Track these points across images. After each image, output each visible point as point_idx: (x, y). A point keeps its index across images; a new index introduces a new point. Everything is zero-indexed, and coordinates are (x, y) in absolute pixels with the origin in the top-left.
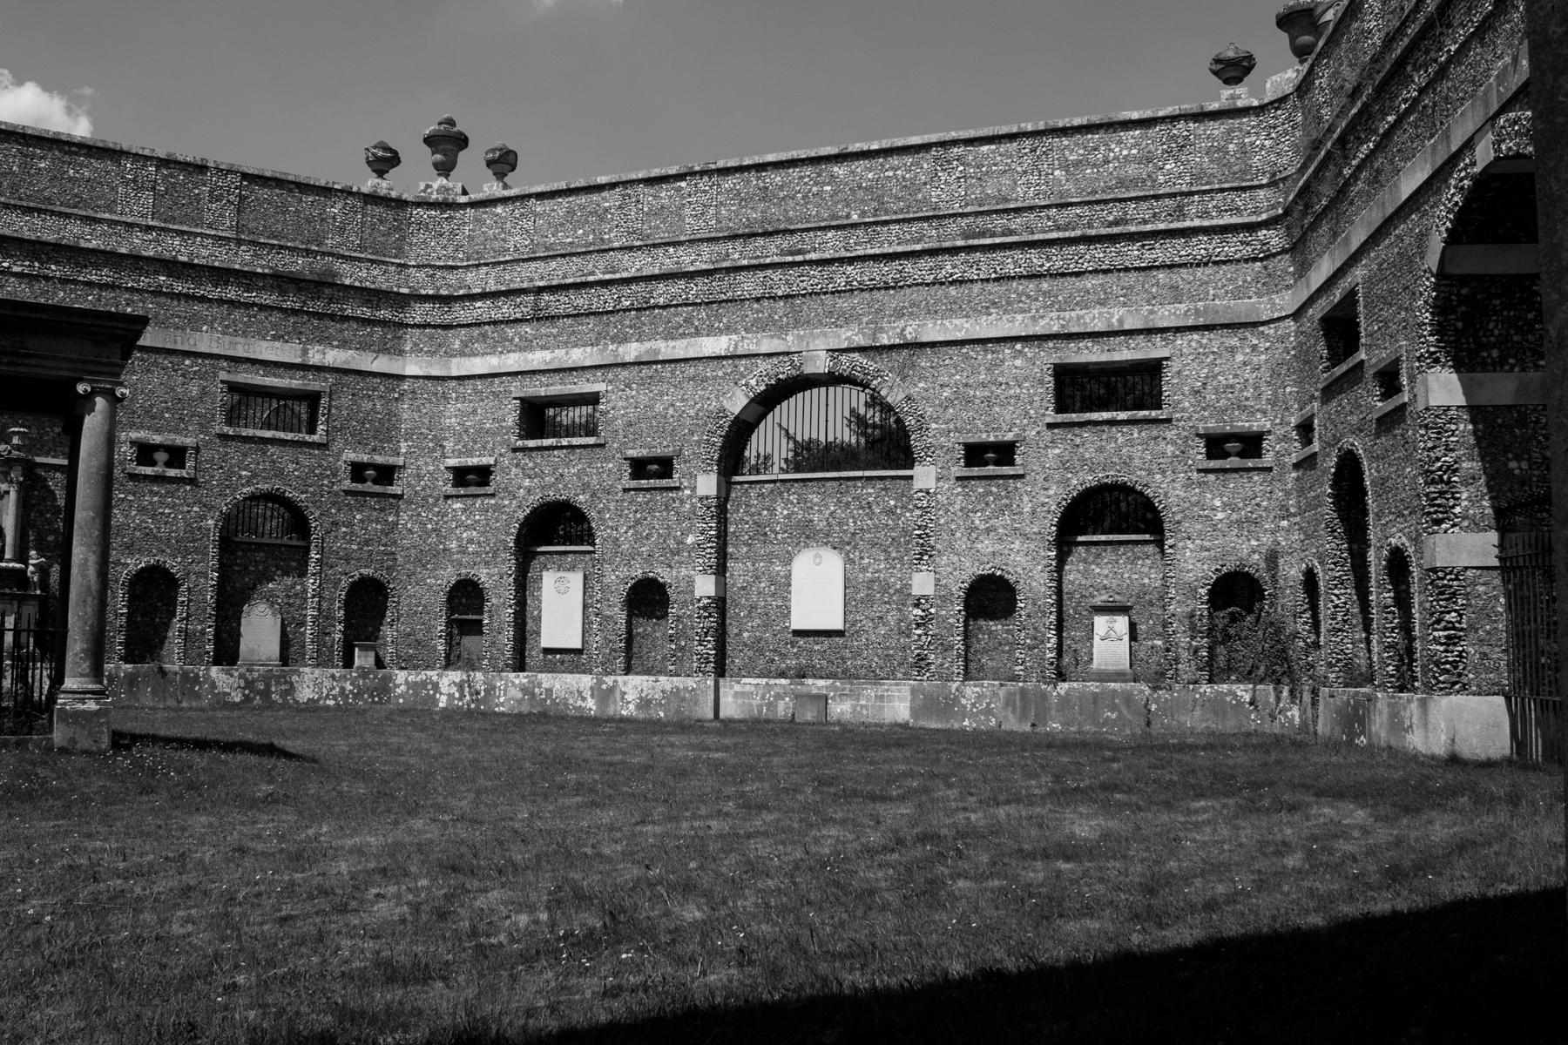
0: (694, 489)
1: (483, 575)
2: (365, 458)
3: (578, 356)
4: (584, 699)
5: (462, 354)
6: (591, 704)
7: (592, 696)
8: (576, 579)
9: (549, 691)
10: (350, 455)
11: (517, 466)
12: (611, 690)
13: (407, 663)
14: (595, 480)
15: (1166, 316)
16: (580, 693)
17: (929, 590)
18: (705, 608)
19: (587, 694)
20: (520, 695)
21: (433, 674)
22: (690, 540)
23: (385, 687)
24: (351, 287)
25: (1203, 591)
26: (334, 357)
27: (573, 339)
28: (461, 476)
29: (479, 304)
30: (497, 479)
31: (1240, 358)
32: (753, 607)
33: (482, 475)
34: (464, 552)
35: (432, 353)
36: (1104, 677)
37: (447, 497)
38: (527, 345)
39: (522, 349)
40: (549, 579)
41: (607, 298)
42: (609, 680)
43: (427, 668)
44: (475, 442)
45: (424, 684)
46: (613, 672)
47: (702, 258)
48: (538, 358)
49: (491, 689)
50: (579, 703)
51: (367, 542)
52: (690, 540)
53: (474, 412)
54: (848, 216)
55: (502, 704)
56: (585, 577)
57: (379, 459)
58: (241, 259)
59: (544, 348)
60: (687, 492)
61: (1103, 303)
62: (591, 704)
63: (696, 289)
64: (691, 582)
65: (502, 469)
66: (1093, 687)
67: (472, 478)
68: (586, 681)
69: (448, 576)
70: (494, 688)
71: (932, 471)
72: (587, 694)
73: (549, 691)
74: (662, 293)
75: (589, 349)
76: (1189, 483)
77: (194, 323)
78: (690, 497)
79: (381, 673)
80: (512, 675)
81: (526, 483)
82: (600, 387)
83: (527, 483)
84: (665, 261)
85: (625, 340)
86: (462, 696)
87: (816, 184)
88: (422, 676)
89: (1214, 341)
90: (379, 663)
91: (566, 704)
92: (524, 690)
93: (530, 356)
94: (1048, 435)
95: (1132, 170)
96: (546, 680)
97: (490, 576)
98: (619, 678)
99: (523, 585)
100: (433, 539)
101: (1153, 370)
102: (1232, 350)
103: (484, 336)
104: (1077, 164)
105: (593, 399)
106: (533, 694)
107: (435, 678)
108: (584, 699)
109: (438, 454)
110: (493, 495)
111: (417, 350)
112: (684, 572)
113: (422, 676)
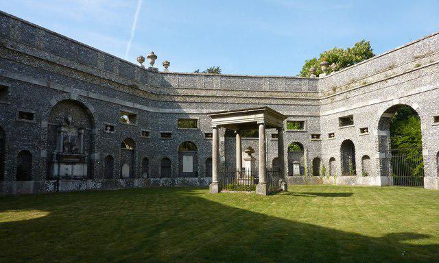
1: (170, 157)
6: (198, 183)
8: (191, 158)
9: (188, 182)
10: (142, 130)
15: (306, 113)
26: (138, 106)
28: (163, 135)
33: (170, 134)
36: (296, 175)
40: (185, 158)
41: (199, 100)
47: (219, 94)
58: (121, 80)
63: (218, 100)
67: (166, 135)
69: (160, 157)
73: (188, 182)
74: (211, 100)
77: (114, 96)
81: (180, 139)
84: (210, 93)
89: (313, 119)
92: (182, 181)
96: (187, 179)
99: (181, 159)
101: (302, 123)
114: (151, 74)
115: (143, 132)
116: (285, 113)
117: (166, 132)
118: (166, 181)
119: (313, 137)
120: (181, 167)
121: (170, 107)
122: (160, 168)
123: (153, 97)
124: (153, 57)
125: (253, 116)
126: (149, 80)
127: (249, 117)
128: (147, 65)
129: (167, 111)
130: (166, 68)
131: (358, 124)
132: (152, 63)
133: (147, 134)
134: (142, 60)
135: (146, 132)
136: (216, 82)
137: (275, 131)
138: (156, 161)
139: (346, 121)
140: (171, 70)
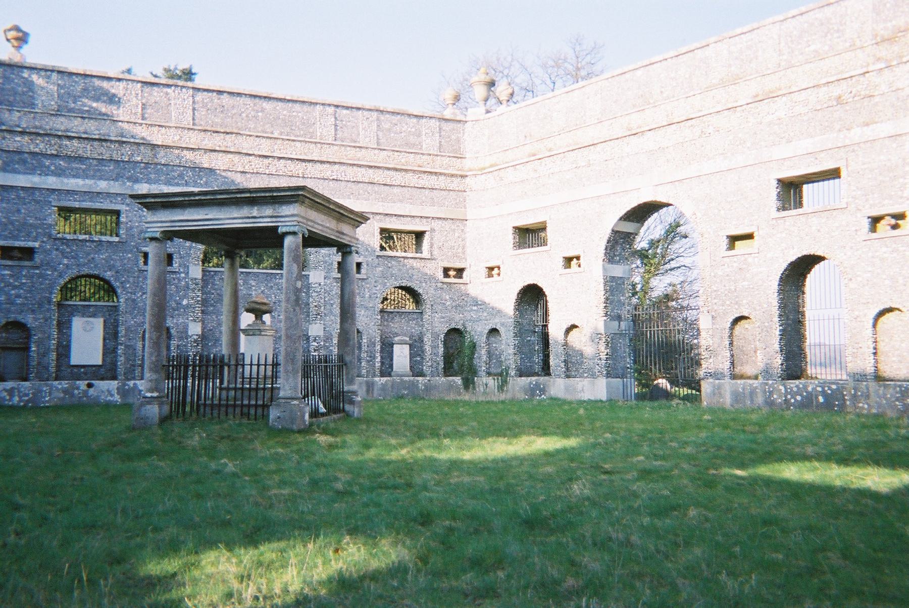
1: (29, 320)
3: (102, 185)
4: (112, 395)
6: (117, 398)
7: (118, 393)
8: (98, 324)
11: (57, 250)
14: (118, 264)
18: (195, 341)
20: (62, 395)
22: (185, 302)
27: (98, 174)
29: (18, 139)
30: (38, 258)
31: (457, 234)
33: (28, 253)
34: (12, 303)
39: (59, 175)
40: (78, 323)
46: (134, 378)
50: (109, 398)
52: (185, 302)
53: (18, 211)
54: (272, 133)
55: (47, 402)
56: (105, 322)
59: (74, 176)
60: (183, 275)
61: (401, 201)
62: (117, 398)
64: (186, 328)
68: (114, 384)
70: (41, 391)
71: (323, 274)
75: (112, 182)
78: (185, 278)
83: (65, 261)
85: (137, 181)
87: (253, 110)
89: (447, 225)
92: (65, 391)
93: (65, 180)
97: (35, 319)
98: (137, 382)
99: (64, 326)
103: (24, 162)
105: (117, 213)
108: (112, 395)
110: (37, 268)
112: (181, 320)
116: (356, 205)
117: (17, 244)
119: (446, 275)
120: (64, 350)
121: (32, 171)
125: (268, 211)
127: (255, 212)
130: (18, 48)
131: (558, 243)
136: (179, 102)
137: (332, 256)
139: (529, 235)
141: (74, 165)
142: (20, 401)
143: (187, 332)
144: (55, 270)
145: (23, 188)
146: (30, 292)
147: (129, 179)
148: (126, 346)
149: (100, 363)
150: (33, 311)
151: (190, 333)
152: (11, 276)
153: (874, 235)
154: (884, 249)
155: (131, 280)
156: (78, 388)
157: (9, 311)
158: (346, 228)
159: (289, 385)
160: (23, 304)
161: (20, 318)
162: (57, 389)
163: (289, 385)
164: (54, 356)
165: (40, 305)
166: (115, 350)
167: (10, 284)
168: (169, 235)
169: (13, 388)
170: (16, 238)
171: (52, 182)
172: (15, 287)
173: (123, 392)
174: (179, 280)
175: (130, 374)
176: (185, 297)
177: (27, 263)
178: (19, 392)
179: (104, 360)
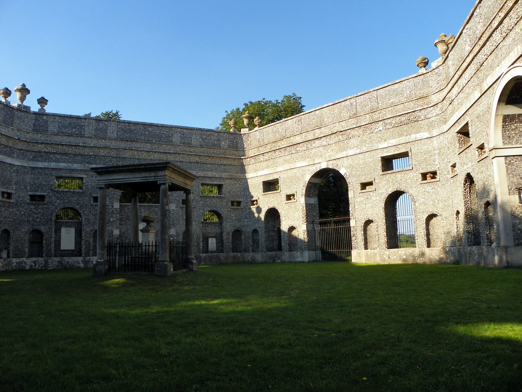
0: (113, 206)
1: (42, 229)
2: (5, 190)
3: (76, 166)
4: (80, 264)
5: (33, 160)
6: (82, 265)
8: (73, 230)
9: (68, 262)
12: (88, 261)
13: (16, 256)
16: (78, 262)
17: (175, 233)
18: (117, 238)
19: (81, 262)
20: (57, 264)
21: (25, 259)
22: (112, 220)
23: (10, 263)
24: (4, 135)
25: (231, 234)
28: (33, 198)
29: (40, 146)
30: (46, 200)
32: (126, 238)
33: (42, 198)
34: (35, 221)
35: (22, 159)
36: (212, 252)
37: (29, 204)
38: (57, 161)
39: (55, 162)
40: (63, 230)
42: (88, 258)
43: (22, 257)
44: (39, 188)
45: (21, 262)
46: (89, 256)
48: (62, 165)
49: (46, 262)
50: (78, 265)
51: (5, 218)
53: (38, 178)
56: (75, 229)
57: (9, 191)
59: (63, 162)
61: (211, 171)
62: (82, 265)
64: (112, 231)
65: (49, 197)
66: (210, 254)
68: (80, 259)
71: (175, 205)
72: (81, 262)
73: (68, 262)
76: (228, 211)
78: (111, 208)
79: (9, 259)
80: (54, 258)
82: (84, 176)
83: (58, 201)
86: (35, 265)
88: (21, 260)
90: (8, 257)
91: (74, 266)
92: (58, 262)
93: (59, 164)
94: (200, 199)
95: (216, 142)
96: (66, 259)
99: (58, 231)
100: (24, 217)
102: (235, 184)
103: (42, 156)
104: (205, 138)
105: (82, 179)
106: (62, 263)
107: (25, 260)
109: (25, 190)
110: (46, 205)
111: (18, 157)
113: (21, 260)
114: (19, 114)
115: (3, 193)
118: (35, 262)
119: (232, 204)
120: (58, 243)
121: (45, 160)
122: (27, 244)
123: (19, 146)
124: (24, 91)
126: (16, 121)
128: (14, 100)
129: (40, 165)
131: (284, 189)
132: (22, 99)
133: (9, 195)
134: (7, 93)
135: (8, 193)
138: (22, 235)
140: (49, 109)
141: (63, 157)
142: (39, 267)
143: (113, 234)
144: (54, 205)
145: (41, 168)
146: (42, 216)
147: (87, 163)
148: (86, 241)
149: (74, 249)
150: (44, 225)
151: (114, 234)
152: (35, 209)
153: (425, 182)
154: (429, 188)
155: (87, 209)
156: (64, 261)
157: (33, 225)
158: (188, 182)
159: (165, 256)
160: (39, 222)
161: (38, 228)
162: (55, 261)
163: (165, 256)
164: (53, 245)
165: (47, 222)
166: (80, 243)
167: (33, 213)
168: (109, 186)
169: (36, 261)
170: (37, 191)
171: (53, 165)
172: (36, 214)
173: (84, 262)
174: (109, 209)
175: (87, 254)
176: (112, 217)
177: (41, 203)
178: (39, 262)
179: (75, 248)
